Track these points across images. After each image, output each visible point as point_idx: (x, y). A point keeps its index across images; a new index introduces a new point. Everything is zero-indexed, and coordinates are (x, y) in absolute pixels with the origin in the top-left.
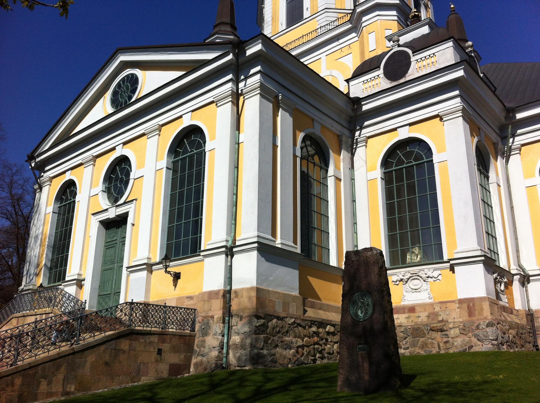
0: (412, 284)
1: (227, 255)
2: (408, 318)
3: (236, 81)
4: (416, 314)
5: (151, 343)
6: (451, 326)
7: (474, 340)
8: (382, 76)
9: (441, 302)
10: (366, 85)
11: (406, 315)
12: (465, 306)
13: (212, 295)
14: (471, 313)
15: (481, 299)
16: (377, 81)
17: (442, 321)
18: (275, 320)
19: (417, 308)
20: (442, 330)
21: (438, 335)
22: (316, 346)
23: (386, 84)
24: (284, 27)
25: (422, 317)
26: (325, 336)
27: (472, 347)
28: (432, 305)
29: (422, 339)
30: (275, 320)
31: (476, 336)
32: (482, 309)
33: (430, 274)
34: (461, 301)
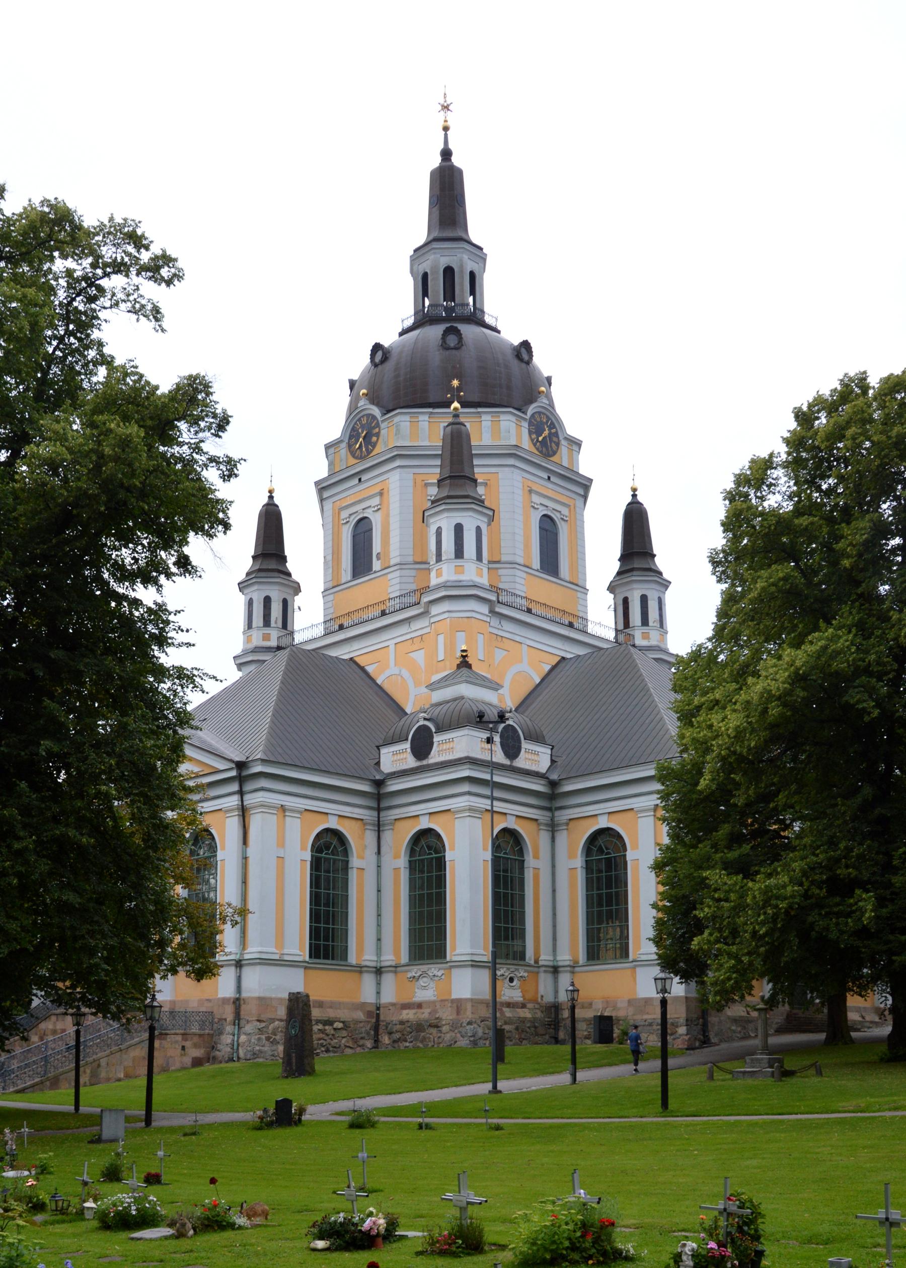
0: (422, 982)
1: (236, 967)
2: (415, 1014)
3: (241, 793)
4: (422, 1011)
5: (176, 1042)
6: (444, 1023)
7: (458, 1035)
8: (409, 750)
9: (442, 1001)
10: (395, 758)
11: (414, 1011)
12: (455, 1005)
13: (225, 1001)
14: (458, 1013)
15: (466, 1000)
16: (402, 756)
17: (437, 1018)
18: (277, 1023)
19: (424, 1005)
20: (437, 1026)
21: (434, 1031)
22: (322, 1041)
23: (411, 762)
24: (349, 578)
25: (425, 1014)
26: (332, 1032)
27: (456, 1042)
28: (434, 1002)
29: (423, 1034)
30: (277, 1023)
31: (460, 1032)
32: (466, 1009)
33: (436, 973)
34: (453, 1001)
